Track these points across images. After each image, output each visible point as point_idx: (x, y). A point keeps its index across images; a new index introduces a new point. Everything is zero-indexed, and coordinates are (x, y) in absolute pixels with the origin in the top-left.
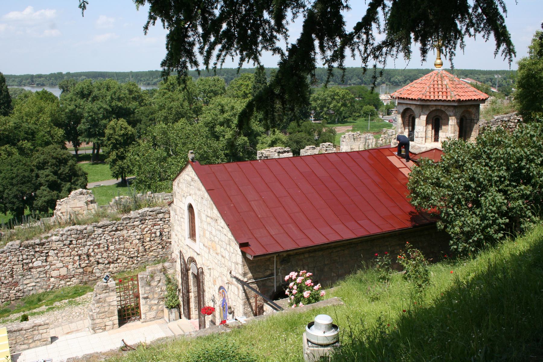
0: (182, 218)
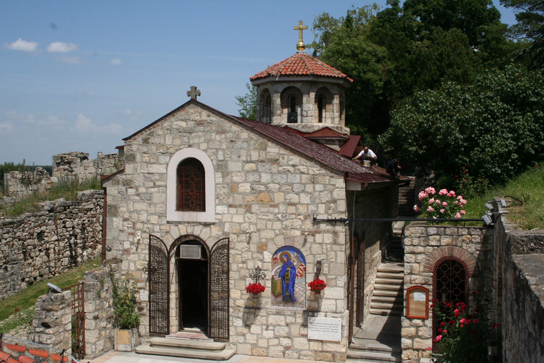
0: (155, 186)
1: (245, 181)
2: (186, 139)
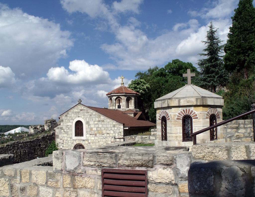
1: (95, 127)
2: (77, 115)
